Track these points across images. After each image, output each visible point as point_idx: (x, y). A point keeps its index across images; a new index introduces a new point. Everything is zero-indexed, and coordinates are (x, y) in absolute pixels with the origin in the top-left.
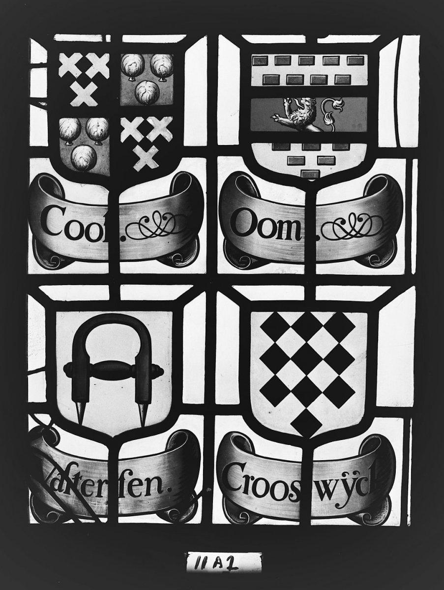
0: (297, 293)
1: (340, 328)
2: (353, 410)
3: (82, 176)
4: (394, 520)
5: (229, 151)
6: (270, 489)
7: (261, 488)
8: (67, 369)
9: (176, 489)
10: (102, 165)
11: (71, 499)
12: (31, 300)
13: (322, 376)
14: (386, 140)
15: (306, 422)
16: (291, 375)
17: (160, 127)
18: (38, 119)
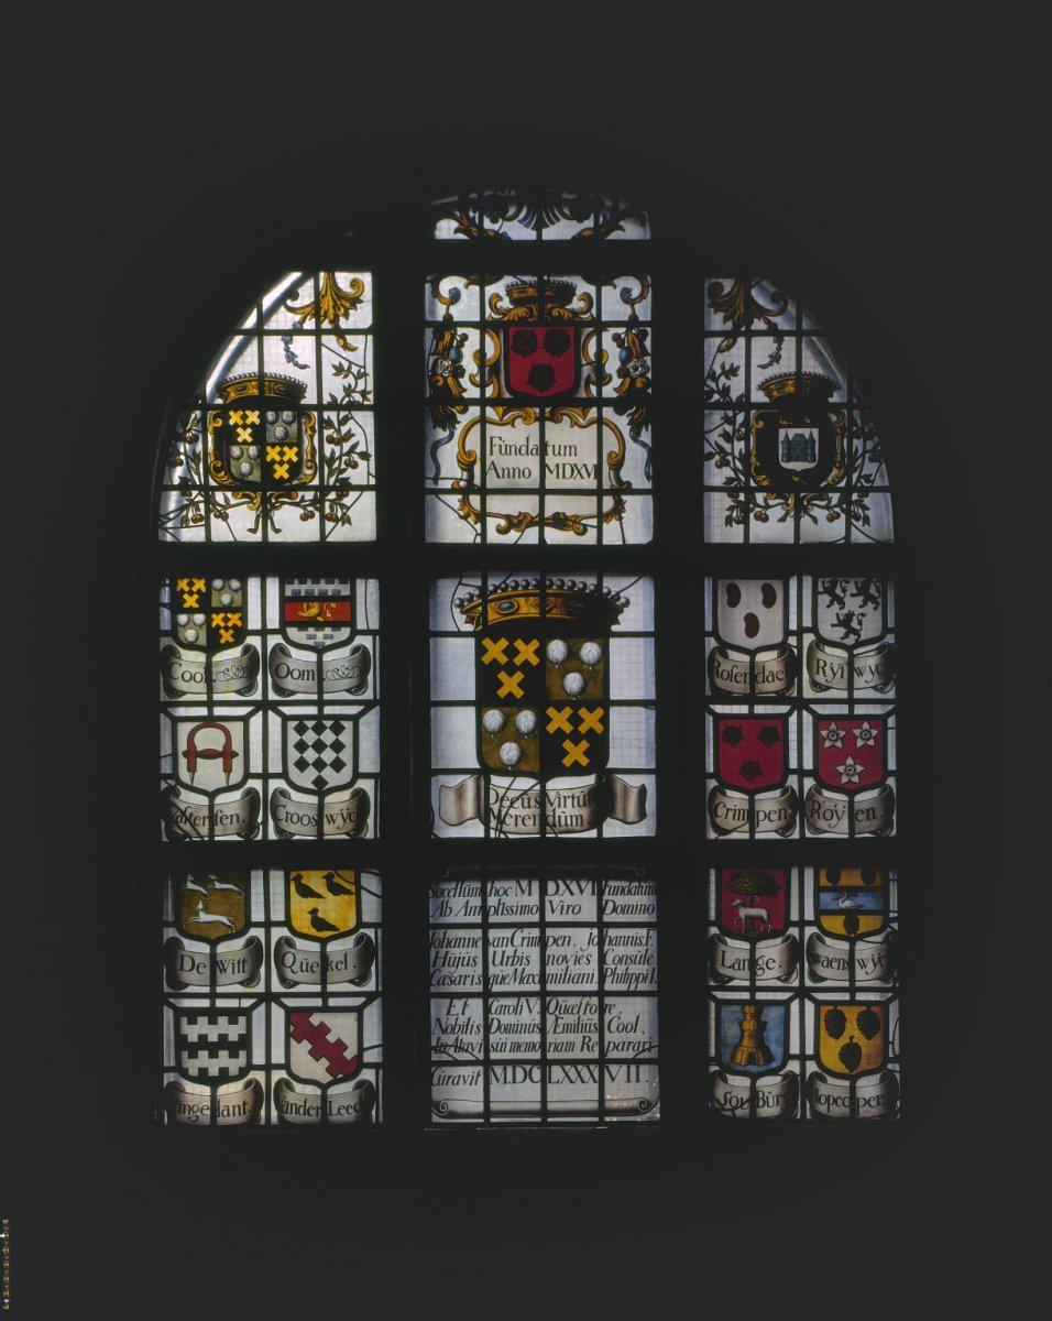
0: (313, 710)
1: (337, 729)
2: (346, 774)
3: (191, 646)
4: (370, 835)
5: (274, 632)
6: (300, 819)
7: (295, 819)
8: (185, 754)
9: (247, 820)
10: (203, 641)
11: (187, 827)
12: (162, 716)
13: (328, 756)
14: (361, 625)
15: (320, 782)
16: (310, 755)
17: (234, 619)
18: (166, 614)
